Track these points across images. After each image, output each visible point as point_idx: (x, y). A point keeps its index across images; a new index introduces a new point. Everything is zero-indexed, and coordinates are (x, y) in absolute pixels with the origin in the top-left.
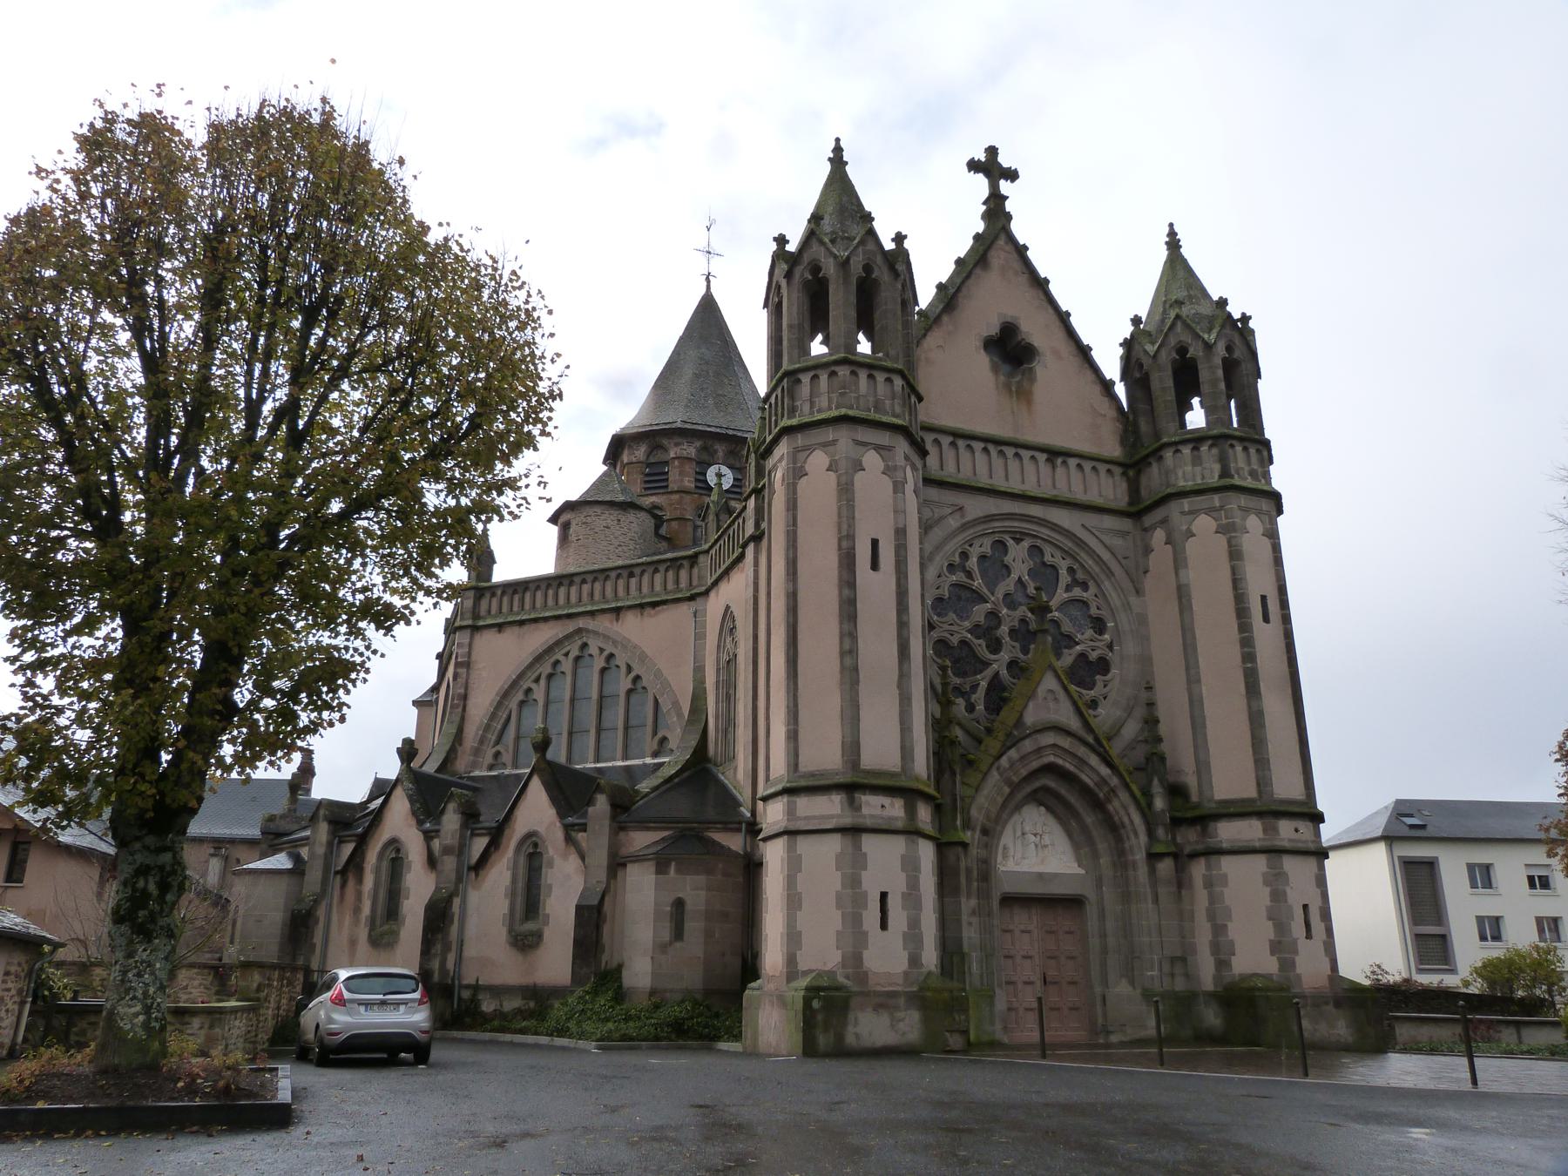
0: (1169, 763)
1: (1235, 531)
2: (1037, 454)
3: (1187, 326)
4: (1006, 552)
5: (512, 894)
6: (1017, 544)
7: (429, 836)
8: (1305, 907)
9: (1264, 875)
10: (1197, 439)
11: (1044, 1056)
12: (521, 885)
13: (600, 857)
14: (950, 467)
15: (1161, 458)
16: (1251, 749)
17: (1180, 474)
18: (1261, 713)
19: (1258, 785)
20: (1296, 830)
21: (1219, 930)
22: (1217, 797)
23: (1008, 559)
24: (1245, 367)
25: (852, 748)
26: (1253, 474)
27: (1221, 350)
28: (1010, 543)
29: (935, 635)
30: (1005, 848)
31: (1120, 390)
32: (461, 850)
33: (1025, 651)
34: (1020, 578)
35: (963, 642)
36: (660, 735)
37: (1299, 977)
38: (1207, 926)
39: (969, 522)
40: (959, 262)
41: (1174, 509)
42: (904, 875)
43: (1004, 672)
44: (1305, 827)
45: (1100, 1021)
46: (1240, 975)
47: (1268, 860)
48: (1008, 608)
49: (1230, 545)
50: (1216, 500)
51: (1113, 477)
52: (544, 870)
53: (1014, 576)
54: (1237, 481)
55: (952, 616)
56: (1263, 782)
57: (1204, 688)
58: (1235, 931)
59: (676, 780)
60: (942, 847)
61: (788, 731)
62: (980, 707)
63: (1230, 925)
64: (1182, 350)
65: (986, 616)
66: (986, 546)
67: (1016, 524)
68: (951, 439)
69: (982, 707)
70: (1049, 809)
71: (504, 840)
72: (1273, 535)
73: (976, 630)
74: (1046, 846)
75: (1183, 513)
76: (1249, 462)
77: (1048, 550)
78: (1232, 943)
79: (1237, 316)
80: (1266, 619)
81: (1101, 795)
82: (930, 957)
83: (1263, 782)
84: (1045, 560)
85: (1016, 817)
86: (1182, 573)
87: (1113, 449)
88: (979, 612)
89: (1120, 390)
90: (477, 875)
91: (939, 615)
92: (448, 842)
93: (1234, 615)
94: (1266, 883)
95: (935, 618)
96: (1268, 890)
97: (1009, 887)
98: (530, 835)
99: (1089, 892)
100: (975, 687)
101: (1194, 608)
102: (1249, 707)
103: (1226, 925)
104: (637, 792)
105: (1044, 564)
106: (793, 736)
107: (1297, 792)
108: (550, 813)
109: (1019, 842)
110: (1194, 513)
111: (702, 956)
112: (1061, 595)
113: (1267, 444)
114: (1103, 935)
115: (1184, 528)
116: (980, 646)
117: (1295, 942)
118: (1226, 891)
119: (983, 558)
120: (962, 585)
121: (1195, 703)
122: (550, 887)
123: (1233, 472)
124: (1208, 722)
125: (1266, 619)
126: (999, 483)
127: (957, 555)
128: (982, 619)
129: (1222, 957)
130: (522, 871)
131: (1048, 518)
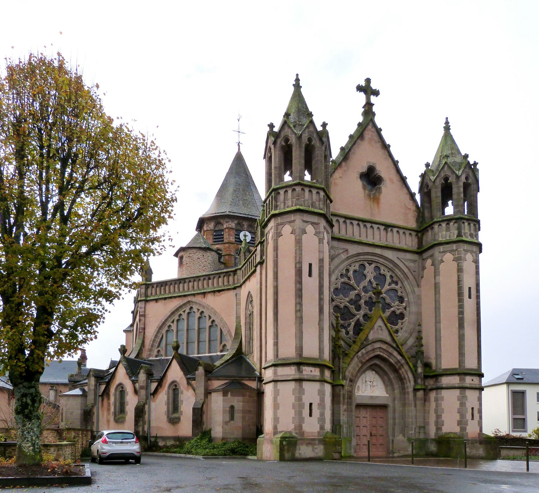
0: (425, 354)
1: (461, 260)
2: (380, 227)
3: (449, 167)
4: (365, 269)
6: (370, 266)
7: (134, 382)
8: (473, 408)
9: (458, 397)
10: (449, 220)
11: (369, 461)
13: (201, 390)
14: (343, 232)
15: (433, 228)
17: (440, 235)
18: (464, 335)
19: (459, 363)
20: (472, 380)
21: (438, 417)
22: (443, 368)
23: (365, 272)
24: (473, 187)
25: (300, 349)
26: (471, 235)
27: (463, 179)
28: (367, 265)
29: (334, 303)
30: (358, 387)
31: (418, 197)
33: (371, 310)
34: (370, 280)
35: (346, 307)
36: (223, 344)
37: (467, 433)
38: (435, 415)
39: (350, 256)
40: (351, 137)
41: (436, 251)
42: (319, 397)
44: (476, 379)
45: (391, 448)
47: (460, 391)
48: (365, 293)
49: (458, 266)
50: (454, 246)
52: (179, 395)
53: (368, 279)
54: (464, 238)
55: (341, 296)
56: (461, 362)
57: (442, 325)
58: (445, 417)
59: (230, 361)
60: (334, 386)
61: (274, 342)
62: (351, 333)
63: (443, 415)
64: (446, 179)
65: (355, 296)
66: (357, 267)
67: (370, 257)
68: (344, 219)
69: (352, 333)
70: (376, 372)
71: (163, 384)
72: (476, 262)
73: (350, 302)
74: (374, 386)
75: (440, 252)
76: (470, 230)
77: (382, 268)
78: (443, 421)
79: (472, 162)
80: (470, 297)
81: (397, 367)
82: (328, 426)
83: (461, 362)
84: (381, 272)
85: (363, 375)
86: (437, 277)
87: (412, 224)
88: (352, 294)
89: (418, 197)
91: (336, 295)
93: (457, 295)
94: (459, 400)
95: (334, 296)
96: (459, 402)
97: (359, 401)
98: (173, 382)
99: (390, 403)
100: (349, 325)
101: (441, 293)
102: (459, 332)
104: (215, 365)
105: (380, 274)
106: (276, 344)
107: (474, 366)
109: (364, 385)
110: (444, 252)
111: (241, 426)
112: (387, 287)
113: (478, 222)
114: (394, 419)
115: (440, 259)
116: (352, 308)
117: (467, 421)
118: (443, 402)
119: (355, 271)
121: (438, 331)
122: (182, 401)
123: (463, 235)
125: (470, 297)
126: (364, 239)
127: (344, 271)
129: (439, 426)
130: (171, 395)
131: (383, 254)
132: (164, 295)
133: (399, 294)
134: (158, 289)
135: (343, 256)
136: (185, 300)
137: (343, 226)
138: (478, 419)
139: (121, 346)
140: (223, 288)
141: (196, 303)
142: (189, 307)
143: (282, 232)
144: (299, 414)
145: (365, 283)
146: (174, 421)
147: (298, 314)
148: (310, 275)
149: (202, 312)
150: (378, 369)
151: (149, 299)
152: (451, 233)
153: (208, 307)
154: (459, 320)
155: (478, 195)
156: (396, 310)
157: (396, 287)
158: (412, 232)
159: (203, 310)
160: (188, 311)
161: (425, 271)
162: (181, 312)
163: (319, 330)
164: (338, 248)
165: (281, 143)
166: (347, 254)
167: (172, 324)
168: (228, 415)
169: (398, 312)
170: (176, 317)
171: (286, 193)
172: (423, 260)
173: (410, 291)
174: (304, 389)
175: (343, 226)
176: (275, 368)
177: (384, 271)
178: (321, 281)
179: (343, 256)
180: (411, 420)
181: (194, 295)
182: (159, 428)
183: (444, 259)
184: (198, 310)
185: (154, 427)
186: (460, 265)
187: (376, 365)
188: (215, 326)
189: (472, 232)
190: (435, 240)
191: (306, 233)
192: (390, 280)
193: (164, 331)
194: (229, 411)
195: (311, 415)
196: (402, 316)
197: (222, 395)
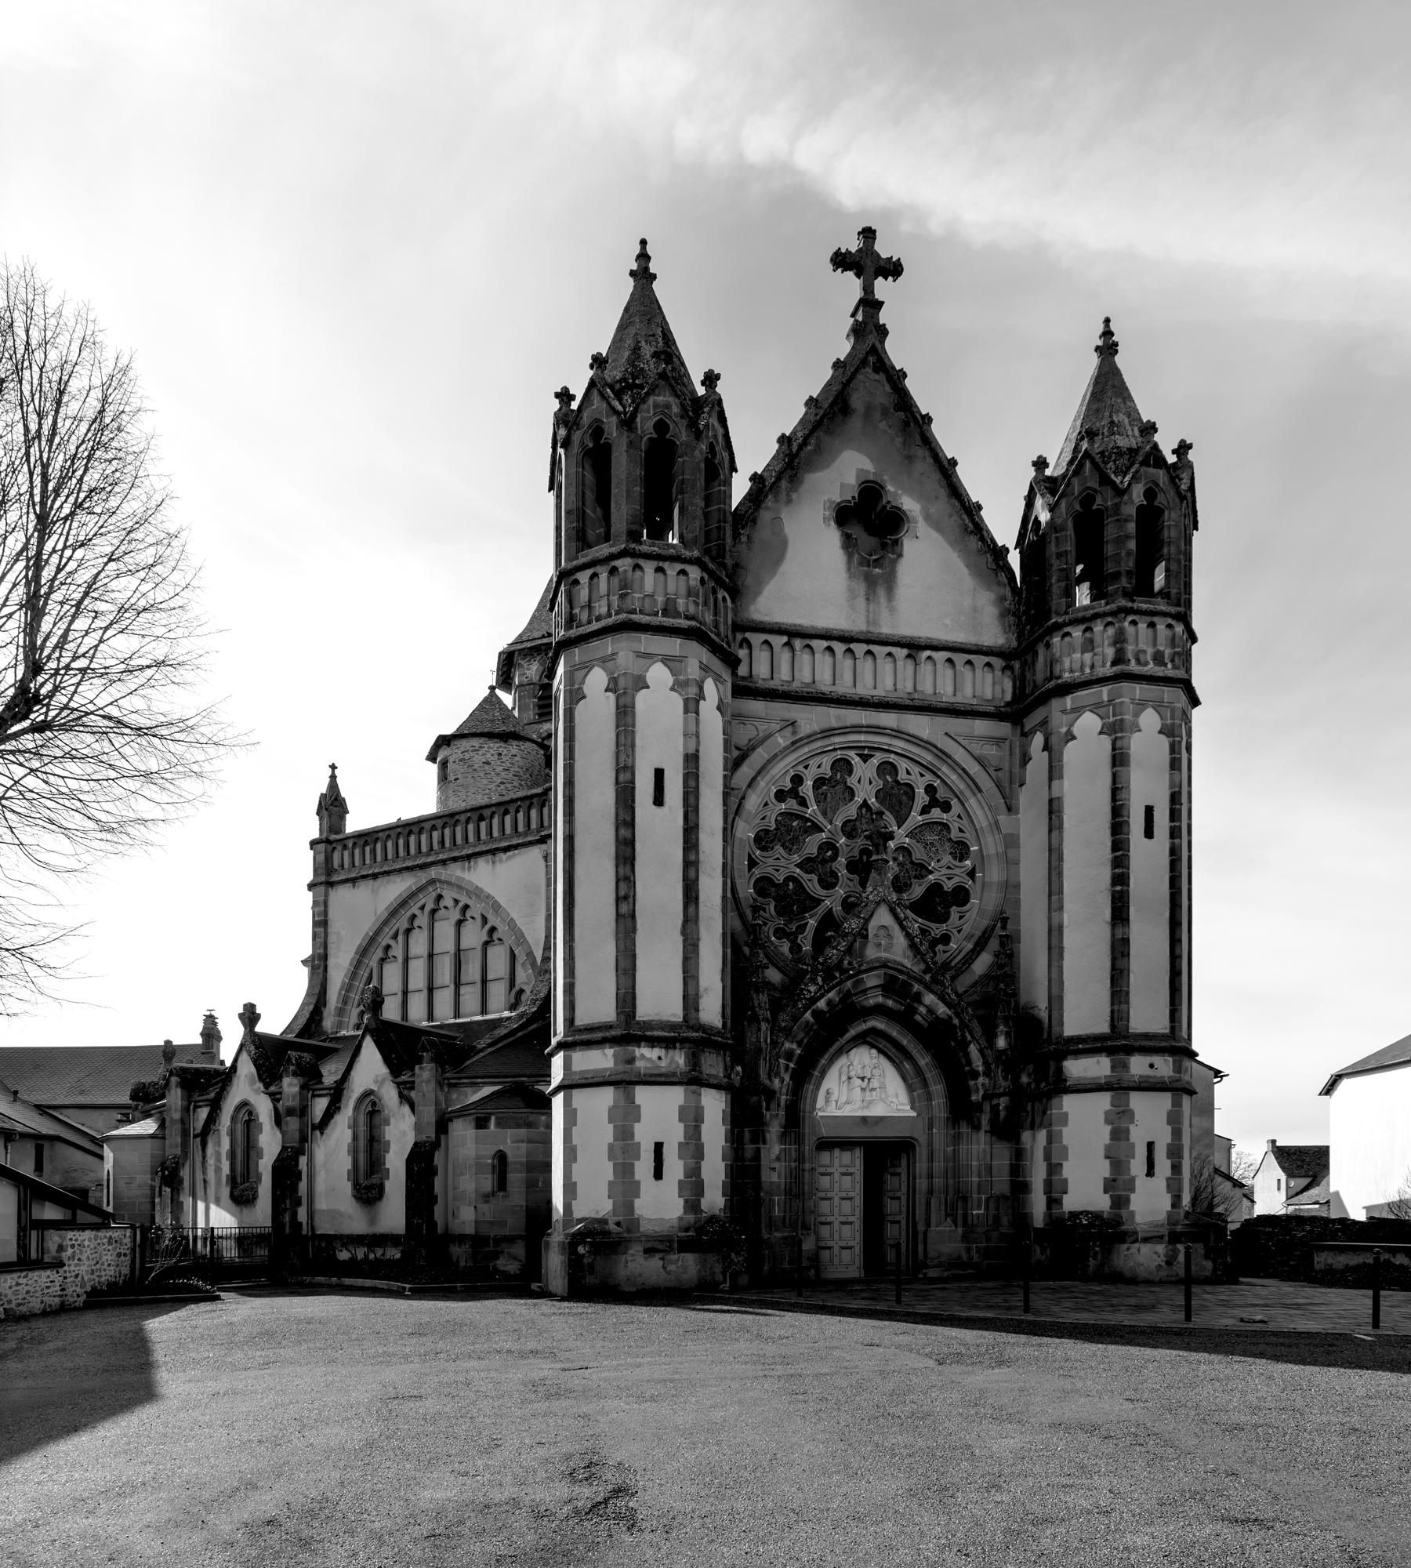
1: (1122, 730)
4: (850, 772)
5: (354, 1151)
6: (865, 762)
7: (275, 1097)
9: (1107, 1113)
12: (362, 1143)
13: (429, 1114)
15: (1048, 645)
16: (1109, 981)
18: (1126, 941)
20: (1151, 1066)
21: (1053, 1169)
23: (852, 781)
28: (856, 760)
29: (757, 872)
31: (1014, 559)
32: (303, 1111)
36: (517, 988)
37: (1132, 1214)
39: (801, 739)
43: (838, 909)
46: (1070, 1213)
47: (1112, 1097)
48: (848, 838)
50: (1104, 692)
51: (993, 671)
53: (859, 799)
54: (1133, 667)
55: (779, 850)
57: (1066, 916)
58: (1069, 1170)
59: (520, 1034)
63: (1065, 1164)
65: (820, 848)
67: (862, 737)
70: (880, 1051)
73: (807, 865)
74: (873, 1089)
77: (903, 765)
78: (1066, 1181)
80: (1149, 833)
85: (842, 1061)
86: (1055, 783)
87: (993, 634)
88: (811, 845)
89: (1014, 559)
90: (322, 1134)
91: (763, 849)
92: (290, 1103)
93: (1108, 832)
94: (1108, 1121)
95: (758, 852)
96: (1109, 1128)
97: (824, 1132)
98: (368, 1093)
100: (802, 928)
101: (1066, 825)
102: (1113, 935)
103: (1061, 1165)
104: (475, 1047)
105: (898, 782)
108: (383, 1070)
109: (845, 1087)
110: (1078, 711)
111: (524, 1204)
114: (930, 1177)
115: (1064, 730)
116: (812, 883)
117: (1133, 1180)
118: (1065, 1130)
119: (819, 782)
120: (792, 814)
121: (1055, 933)
122: (388, 1143)
123: (1130, 656)
124: (1066, 954)
125: (1149, 833)
126: (844, 687)
127: (788, 779)
128: (815, 851)
129: (1054, 1195)
130: (362, 1128)
132: (371, 867)
133: (954, 834)
134: (357, 852)
135: (780, 740)
136: (423, 877)
137: (784, 657)
138: (1168, 1173)
139: (245, 1005)
140: (514, 842)
141: (449, 883)
142: (434, 894)
143: (586, 689)
144: (624, 1171)
145: (850, 811)
146: (368, 1191)
147: (624, 908)
148: (659, 800)
149: (466, 907)
150: (883, 1044)
151: (335, 878)
152: (1095, 655)
153: (478, 893)
154: (1113, 902)
155: (1194, 539)
156: (944, 878)
157: (945, 816)
158: (993, 660)
159: (469, 902)
160: (430, 906)
161: (1029, 766)
162: (415, 910)
163: (684, 947)
165: (582, 443)
166: (794, 733)
167: (392, 943)
168: (490, 1176)
169: (948, 886)
170: (402, 923)
171: (595, 580)
172: (1024, 734)
173: (984, 824)
174: (639, 1107)
175: (784, 657)
176: (567, 1053)
177: (908, 773)
178: (691, 816)
179: (780, 740)
180: (975, 1179)
181: (443, 862)
182: (334, 1214)
183: (1075, 730)
184: (456, 901)
185: (323, 1211)
186: (1119, 744)
187: (873, 1031)
188: (497, 941)
189: (1162, 649)
190: (1051, 677)
191: (648, 687)
192: (927, 798)
193: (373, 963)
194: (493, 1167)
195: (658, 1174)
196: (961, 896)
197: (473, 1124)
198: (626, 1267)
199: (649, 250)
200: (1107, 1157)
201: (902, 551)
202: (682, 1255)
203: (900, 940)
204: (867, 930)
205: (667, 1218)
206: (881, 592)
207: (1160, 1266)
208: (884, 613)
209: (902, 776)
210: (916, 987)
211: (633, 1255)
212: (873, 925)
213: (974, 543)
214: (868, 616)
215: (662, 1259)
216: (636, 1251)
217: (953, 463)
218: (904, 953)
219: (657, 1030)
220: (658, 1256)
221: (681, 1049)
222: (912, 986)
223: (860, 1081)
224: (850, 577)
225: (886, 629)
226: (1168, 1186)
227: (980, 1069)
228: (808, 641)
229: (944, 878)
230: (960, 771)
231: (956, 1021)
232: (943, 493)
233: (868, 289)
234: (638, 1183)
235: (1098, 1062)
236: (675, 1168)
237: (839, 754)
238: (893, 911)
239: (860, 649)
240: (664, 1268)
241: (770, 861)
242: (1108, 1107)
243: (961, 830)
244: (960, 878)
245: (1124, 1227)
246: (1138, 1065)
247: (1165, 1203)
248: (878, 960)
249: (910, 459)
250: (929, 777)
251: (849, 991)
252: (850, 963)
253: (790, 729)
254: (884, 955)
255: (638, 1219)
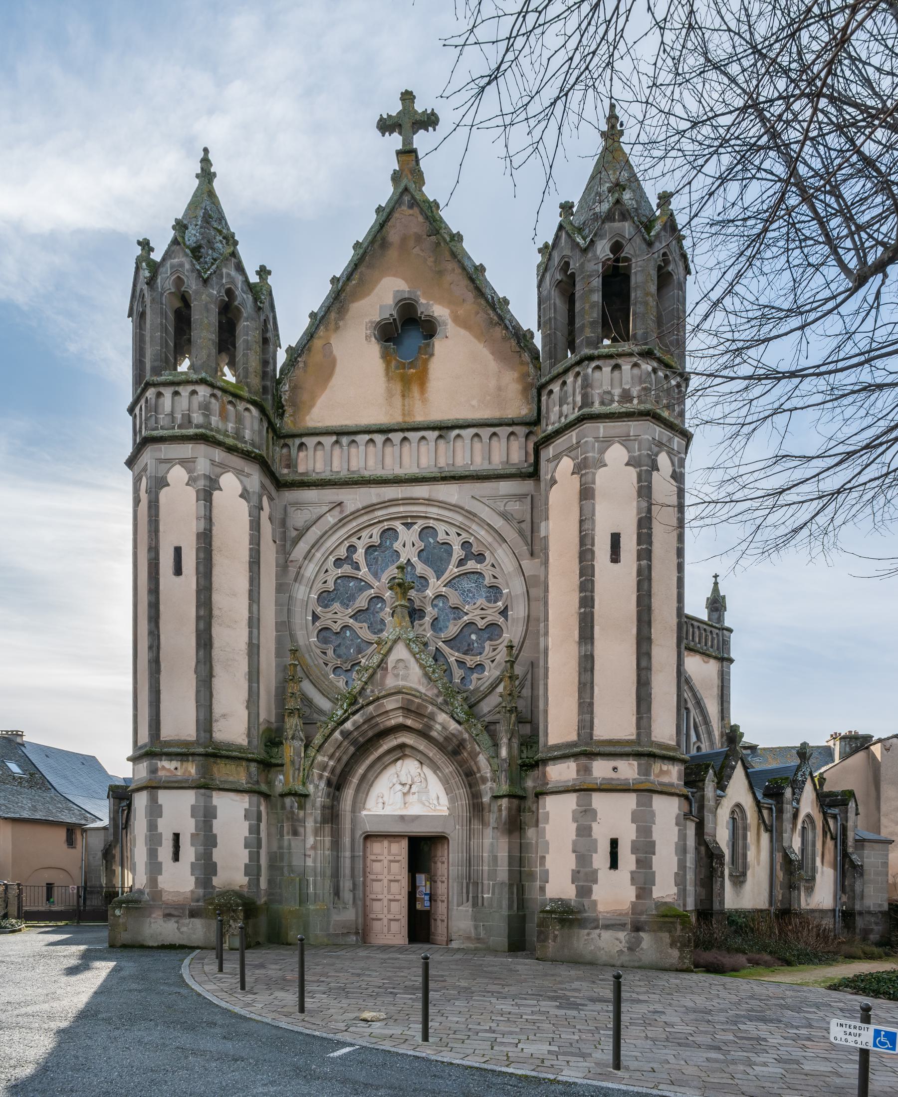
6: (409, 529)
9: (574, 812)
23: (397, 546)
28: (400, 528)
37: (595, 903)
47: (578, 797)
55: (336, 606)
57: (550, 639)
84: (438, 539)
94: (575, 820)
96: (575, 825)
117: (596, 872)
118: (548, 827)
119: (370, 549)
131: (435, 496)
164: (319, 504)
166: (341, 512)
174: (161, 806)
195: (176, 857)
198: (150, 926)
199: (211, 157)
200: (574, 851)
201: (433, 350)
202: (192, 920)
203: (415, 671)
204: (386, 663)
205: (182, 891)
206: (415, 390)
207: (621, 952)
208: (418, 404)
209: (441, 537)
210: (430, 708)
211: (155, 918)
212: (392, 660)
213: (499, 332)
214: (403, 410)
215: (177, 922)
216: (157, 914)
217: (481, 269)
218: (419, 681)
219: (174, 747)
220: (174, 920)
221: (193, 761)
222: (427, 707)
223: (400, 787)
224: (388, 380)
225: (419, 417)
226: (632, 879)
227: (488, 775)
228: (353, 437)
229: (478, 618)
230: (486, 527)
231: (466, 736)
232: (470, 296)
233: (407, 141)
234: (161, 863)
235: (568, 767)
236: (189, 853)
237: (386, 525)
238: (408, 646)
239: (396, 437)
240: (178, 929)
241: (330, 615)
242: (574, 807)
243: (495, 577)
244: (493, 616)
245: (585, 915)
246: (601, 769)
247: (629, 894)
248: (395, 687)
249: (440, 273)
250: (464, 535)
251: (371, 713)
252: (372, 691)
253: (338, 509)
254: (401, 683)
255: (161, 891)
